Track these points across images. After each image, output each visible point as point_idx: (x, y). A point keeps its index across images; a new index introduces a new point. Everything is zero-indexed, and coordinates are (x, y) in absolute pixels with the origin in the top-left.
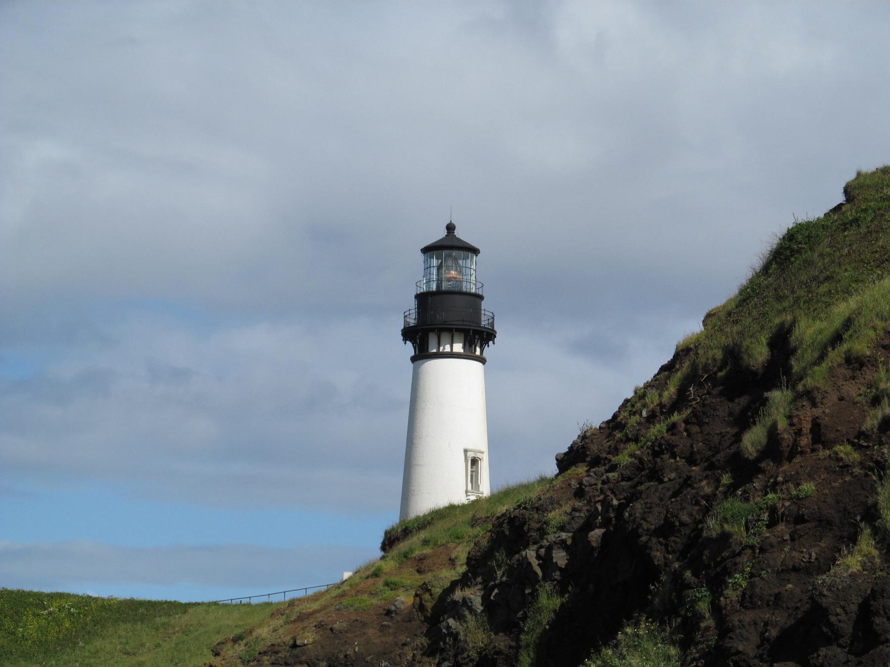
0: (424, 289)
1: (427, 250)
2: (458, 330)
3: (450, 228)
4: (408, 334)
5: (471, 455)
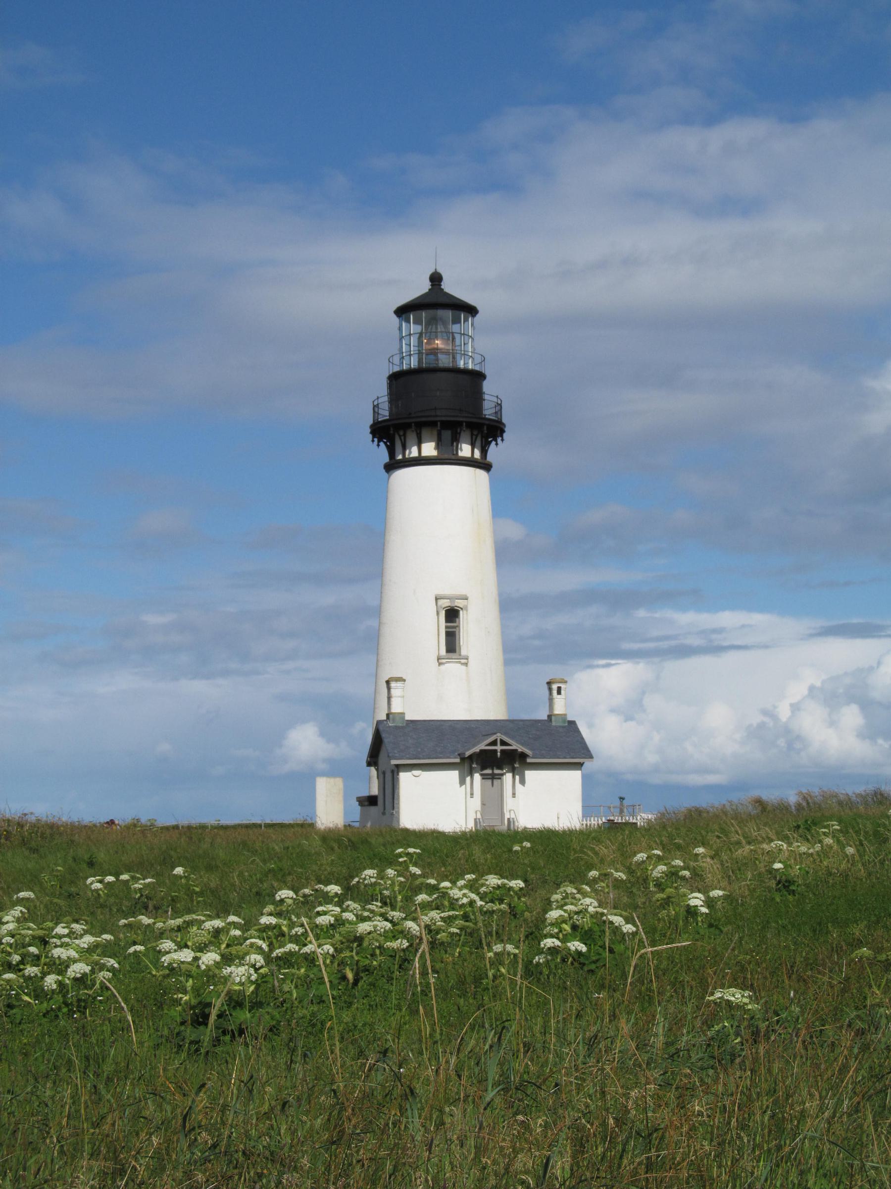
2: (431, 424)
3: (436, 279)
5: (446, 603)
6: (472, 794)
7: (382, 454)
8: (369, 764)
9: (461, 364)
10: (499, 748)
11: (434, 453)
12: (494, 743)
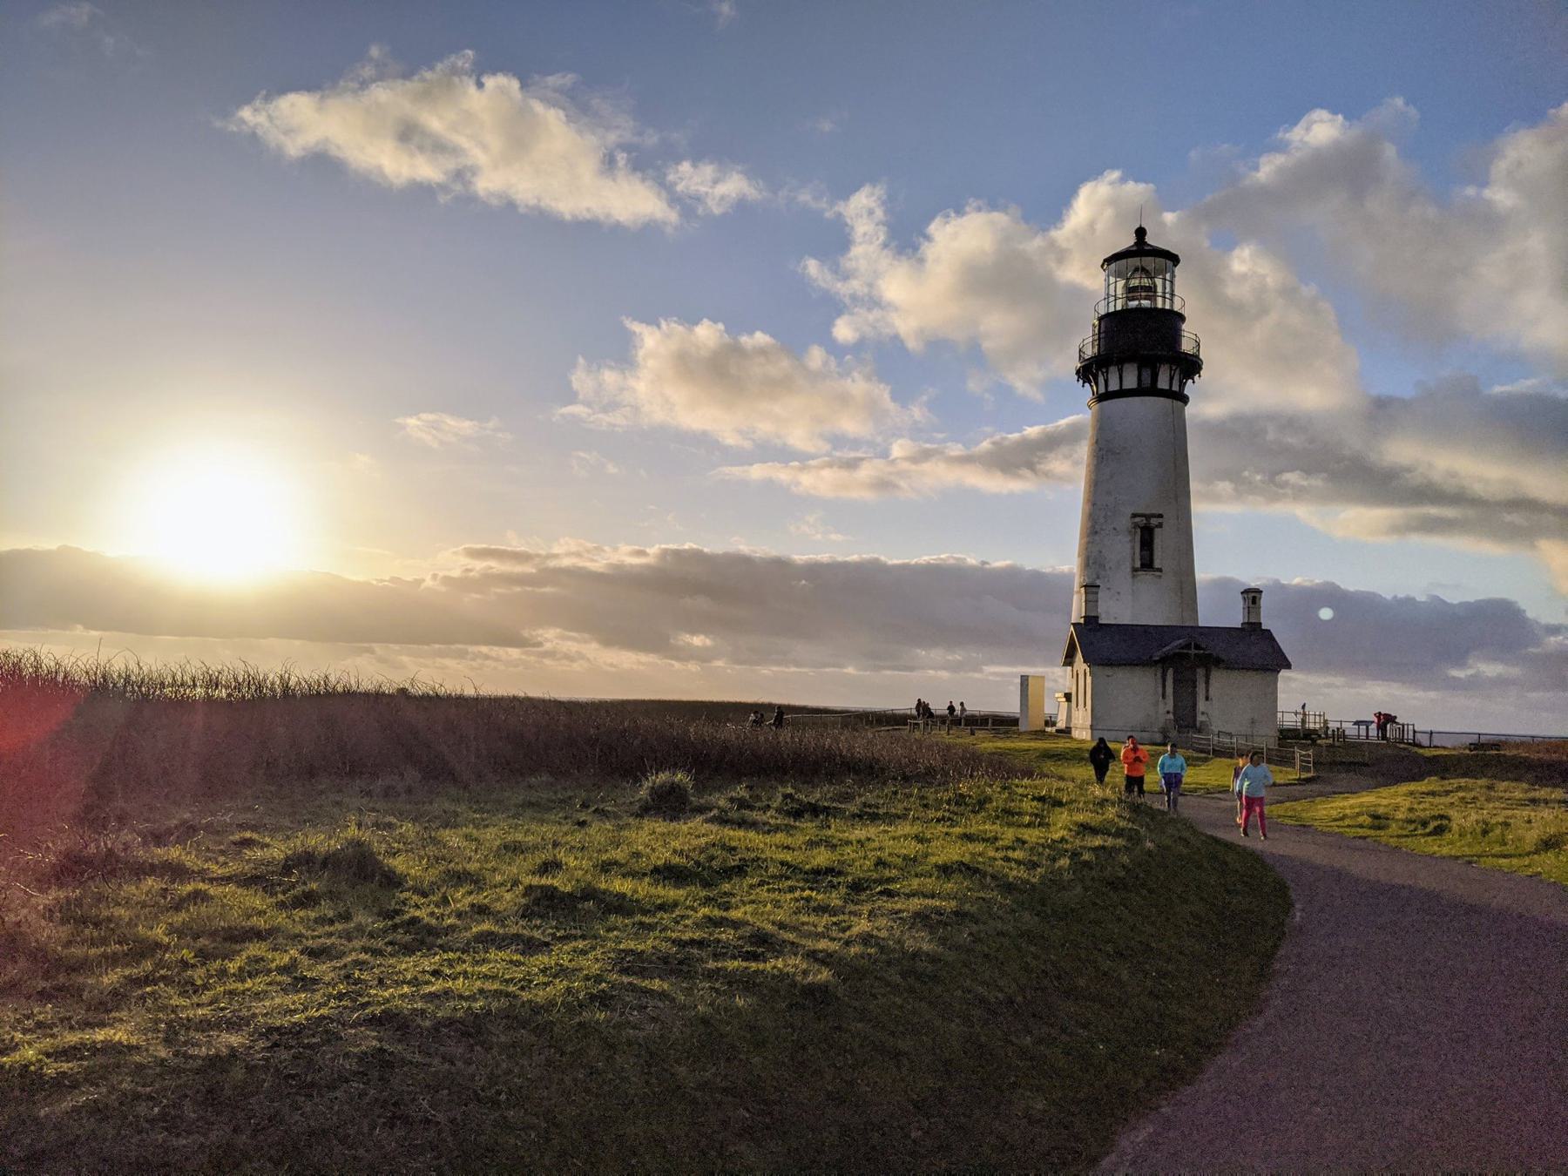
3: (1141, 233)
6: (1164, 696)
7: (1087, 392)
9: (1160, 305)
10: (1193, 651)
12: (1188, 646)
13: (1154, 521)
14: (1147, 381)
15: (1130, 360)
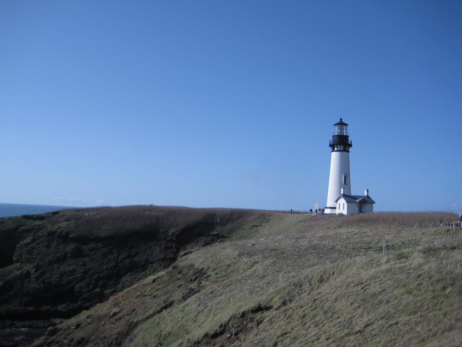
0: (334, 135)
1: (335, 125)
3: (341, 119)
4: (331, 146)
5: (345, 175)
6: (358, 208)
8: (335, 202)
11: (343, 150)
12: (363, 199)
13: (347, 175)
14: (344, 149)
15: (342, 145)
